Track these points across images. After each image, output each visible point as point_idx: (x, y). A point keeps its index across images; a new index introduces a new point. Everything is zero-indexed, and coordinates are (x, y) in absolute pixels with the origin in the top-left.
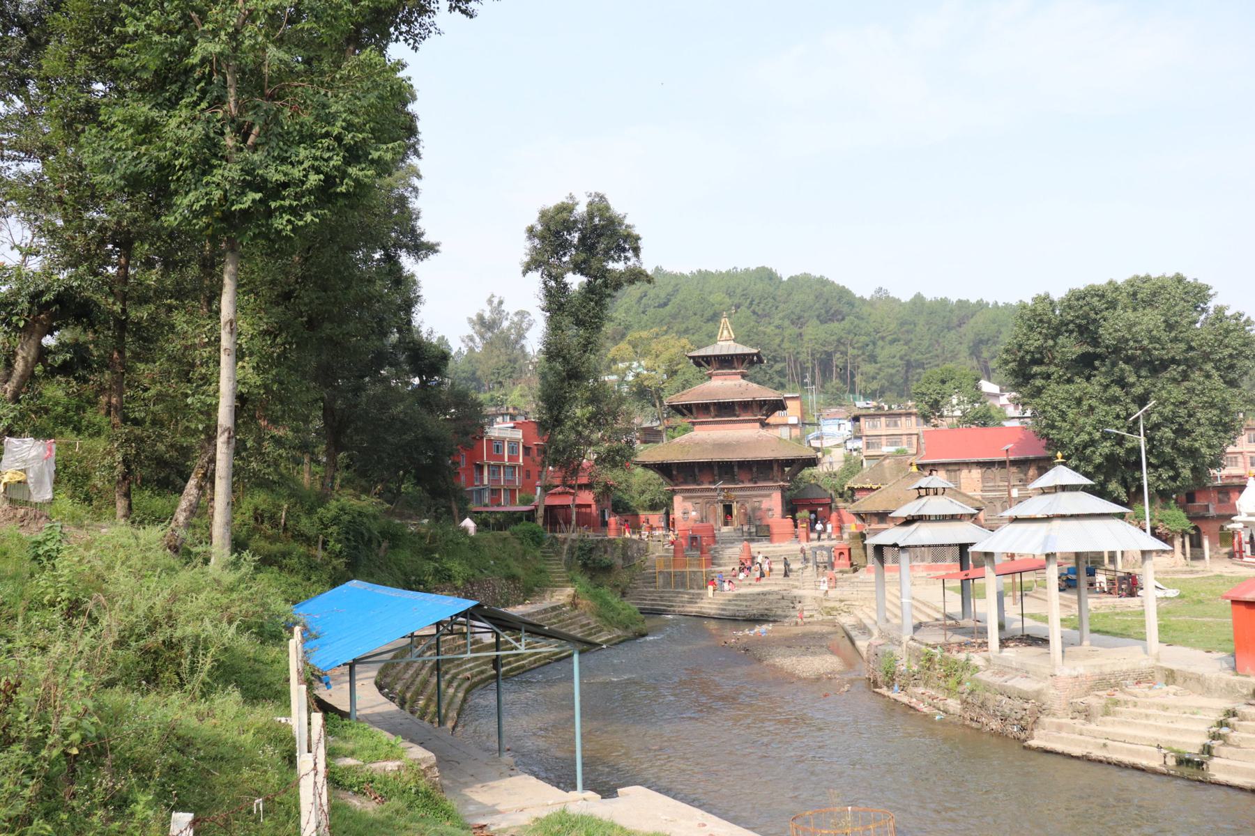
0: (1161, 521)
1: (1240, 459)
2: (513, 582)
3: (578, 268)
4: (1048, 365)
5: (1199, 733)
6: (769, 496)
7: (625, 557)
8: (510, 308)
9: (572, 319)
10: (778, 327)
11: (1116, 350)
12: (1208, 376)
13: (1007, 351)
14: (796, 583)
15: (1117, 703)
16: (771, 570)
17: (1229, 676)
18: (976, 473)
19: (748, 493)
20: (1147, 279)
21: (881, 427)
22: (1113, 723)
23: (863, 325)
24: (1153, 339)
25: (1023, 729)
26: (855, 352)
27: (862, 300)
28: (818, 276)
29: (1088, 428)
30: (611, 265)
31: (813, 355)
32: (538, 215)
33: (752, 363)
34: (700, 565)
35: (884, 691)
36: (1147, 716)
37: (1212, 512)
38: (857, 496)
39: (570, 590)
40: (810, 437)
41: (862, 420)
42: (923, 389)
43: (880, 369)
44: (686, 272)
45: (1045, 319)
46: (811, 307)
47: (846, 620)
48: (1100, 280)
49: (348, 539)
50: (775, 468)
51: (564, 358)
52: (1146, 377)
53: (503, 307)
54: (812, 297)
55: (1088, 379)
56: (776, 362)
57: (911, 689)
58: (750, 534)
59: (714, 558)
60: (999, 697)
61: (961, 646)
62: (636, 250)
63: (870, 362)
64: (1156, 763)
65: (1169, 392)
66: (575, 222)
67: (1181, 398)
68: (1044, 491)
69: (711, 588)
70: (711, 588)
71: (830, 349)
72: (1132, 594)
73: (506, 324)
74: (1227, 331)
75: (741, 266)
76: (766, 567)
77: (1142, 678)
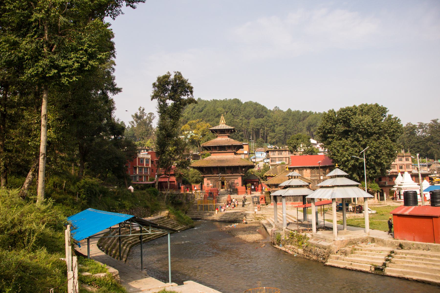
0: (370, 187)
1: (396, 166)
3: (171, 98)
5: (382, 259)
7: (187, 200)
8: (147, 112)
9: (168, 116)
10: (241, 120)
11: (356, 129)
12: (386, 138)
13: (319, 129)
14: (247, 209)
15: (355, 249)
16: (238, 204)
17: (391, 240)
18: (309, 171)
20: (366, 105)
21: (276, 155)
22: (354, 256)
23: (270, 119)
24: (368, 126)
25: (324, 259)
26: (268, 128)
27: (270, 110)
28: (255, 102)
29: (347, 156)
30: (182, 97)
31: (253, 129)
32: (157, 79)
33: (232, 132)
34: (213, 203)
35: (277, 246)
36: (365, 254)
37: (387, 184)
38: (268, 179)
39: (167, 212)
40: (252, 158)
41: (270, 152)
42: (291, 142)
43: (276, 135)
44: (209, 100)
45: (332, 118)
46: (252, 113)
47: (264, 222)
48: (351, 105)
49: (88, 193)
50: (239, 169)
51: (166, 129)
52: (366, 138)
53: (144, 111)
54: (253, 109)
55: (347, 139)
56: (240, 132)
57: (286, 246)
58: (230, 192)
59: (218, 200)
60: (316, 248)
61: (303, 231)
62: (192, 92)
63: (273, 132)
64: (368, 270)
65: (373, 144)
66: (170, 82)
67: (377, 146)
68: (331, 177)
69: (217, 210)
70: (217, 210)
71: (258, 127)
72: (361, 212)
73: (145, 117)
74: (392, 123)
75: (228, 98)
76: (236, 203)
77: (364, 241)
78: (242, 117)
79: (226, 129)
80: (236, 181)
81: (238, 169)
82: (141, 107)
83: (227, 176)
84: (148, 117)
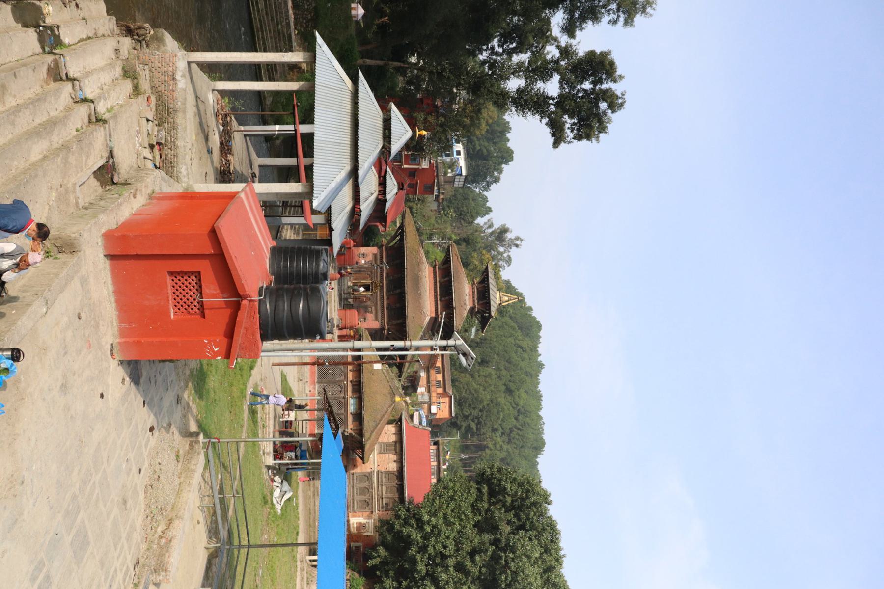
4: (489, 501)
6: (376, 319)
8: (513, 251)
10: (501, 446)
18: (393, 467)
19: (379, 303)
24: (515, 573)
41: (435, 447)
52: (480, 572)
53: (514, 248)
56: (477, 425)
62: (578, 137)
73: (501, 249)
75: (545, 427)
78: (507, 451)
80: (370, 316)
82: (521, 240)
83: (382, 297)
84: (502, 254)
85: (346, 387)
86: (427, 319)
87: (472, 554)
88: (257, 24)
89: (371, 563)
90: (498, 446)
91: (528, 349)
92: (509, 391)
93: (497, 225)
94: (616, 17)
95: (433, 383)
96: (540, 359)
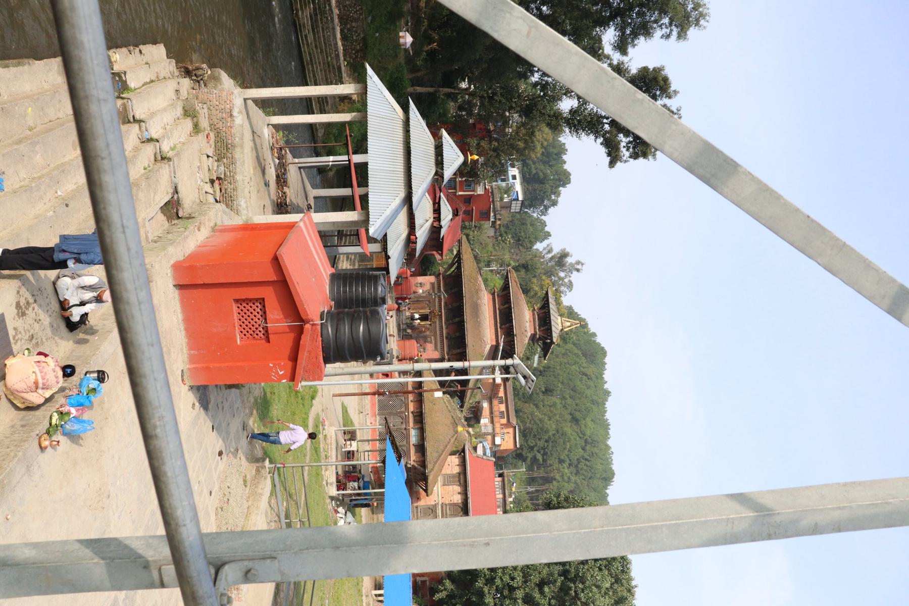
2: (361, 50)
6: (436, 349)
8: (575, 277)
10: (569, 478)
19: (438, 333)
41: (500, 479)
50: (459, 351)
53: (575, 273)
56: (543, 455)
62: (635, 156)
73: (562, 274)
75: (614, 457)
78: (575, 483)
79: (551, 329)
81: (458, 348)
82: (582, 264)
84: (563, 279)
85: (407, 418)
86: (488, 348)
87: (541, 585)
88: (306, 58)
89: (437, 596)
90: (566, 478)
91: (594, 378)
92: (575, 420)
93: (556, 250)
94: (668, 31)
95: (496, 413)
96: (606, 386)
